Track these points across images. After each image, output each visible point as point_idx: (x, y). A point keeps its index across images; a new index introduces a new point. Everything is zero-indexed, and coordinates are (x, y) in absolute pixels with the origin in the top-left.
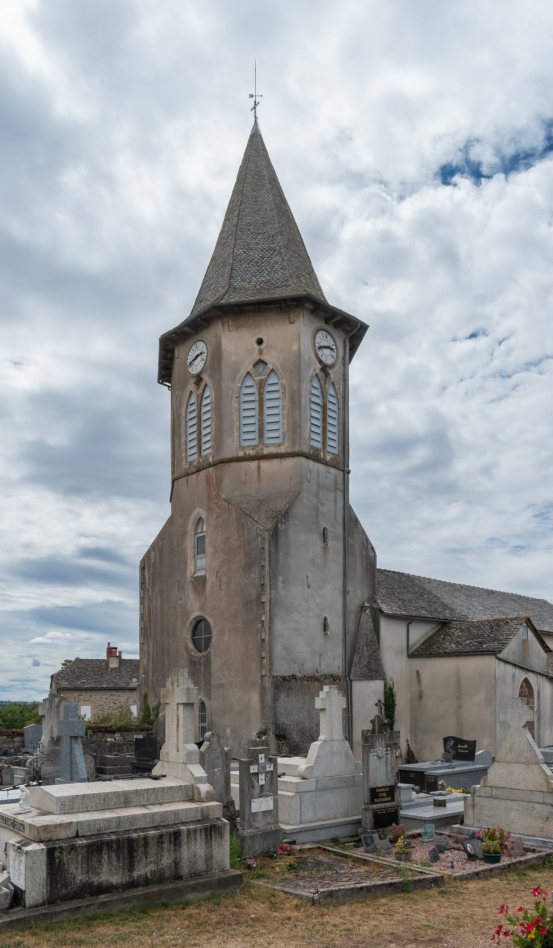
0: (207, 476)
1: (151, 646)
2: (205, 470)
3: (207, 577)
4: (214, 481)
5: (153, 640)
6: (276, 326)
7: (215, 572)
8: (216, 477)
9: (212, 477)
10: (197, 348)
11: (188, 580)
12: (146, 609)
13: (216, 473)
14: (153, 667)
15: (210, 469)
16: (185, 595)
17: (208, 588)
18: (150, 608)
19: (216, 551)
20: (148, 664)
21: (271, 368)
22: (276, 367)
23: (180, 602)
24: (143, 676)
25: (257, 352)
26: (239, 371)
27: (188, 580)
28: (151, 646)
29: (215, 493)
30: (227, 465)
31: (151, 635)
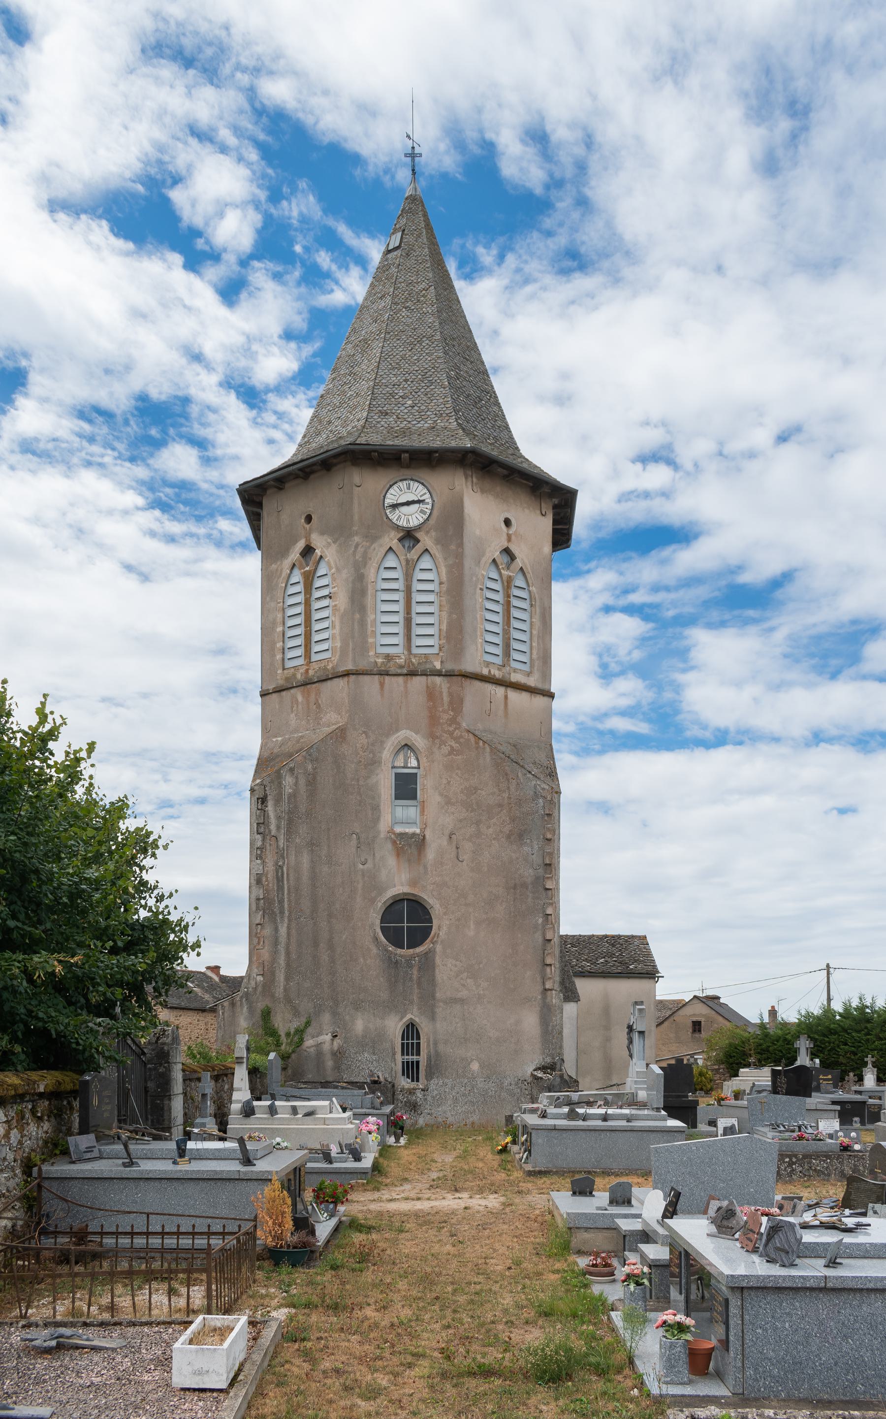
0: (427, 687)
1: (283, 930)
2: (425, 677)
3: (427, 837)
4: (446, 699)
5: (289, 920)
7: (447, 832)
8: (450, 694)
9: (441, 693)
11: (382, 835)
12: (270, 867)
13: (449, 688)
14: (288, 965)
15: (438, 680)
16: (374, 859)
17: (431, 854)
18: (281, 867)
19: (448, 802)
20: (274, 960)
23: (361, 866)
24: (260, 978)
27: (382, 835)
28: (283, 930)
29: (445, 717)
30: (468, 680)
31: (282, 912)
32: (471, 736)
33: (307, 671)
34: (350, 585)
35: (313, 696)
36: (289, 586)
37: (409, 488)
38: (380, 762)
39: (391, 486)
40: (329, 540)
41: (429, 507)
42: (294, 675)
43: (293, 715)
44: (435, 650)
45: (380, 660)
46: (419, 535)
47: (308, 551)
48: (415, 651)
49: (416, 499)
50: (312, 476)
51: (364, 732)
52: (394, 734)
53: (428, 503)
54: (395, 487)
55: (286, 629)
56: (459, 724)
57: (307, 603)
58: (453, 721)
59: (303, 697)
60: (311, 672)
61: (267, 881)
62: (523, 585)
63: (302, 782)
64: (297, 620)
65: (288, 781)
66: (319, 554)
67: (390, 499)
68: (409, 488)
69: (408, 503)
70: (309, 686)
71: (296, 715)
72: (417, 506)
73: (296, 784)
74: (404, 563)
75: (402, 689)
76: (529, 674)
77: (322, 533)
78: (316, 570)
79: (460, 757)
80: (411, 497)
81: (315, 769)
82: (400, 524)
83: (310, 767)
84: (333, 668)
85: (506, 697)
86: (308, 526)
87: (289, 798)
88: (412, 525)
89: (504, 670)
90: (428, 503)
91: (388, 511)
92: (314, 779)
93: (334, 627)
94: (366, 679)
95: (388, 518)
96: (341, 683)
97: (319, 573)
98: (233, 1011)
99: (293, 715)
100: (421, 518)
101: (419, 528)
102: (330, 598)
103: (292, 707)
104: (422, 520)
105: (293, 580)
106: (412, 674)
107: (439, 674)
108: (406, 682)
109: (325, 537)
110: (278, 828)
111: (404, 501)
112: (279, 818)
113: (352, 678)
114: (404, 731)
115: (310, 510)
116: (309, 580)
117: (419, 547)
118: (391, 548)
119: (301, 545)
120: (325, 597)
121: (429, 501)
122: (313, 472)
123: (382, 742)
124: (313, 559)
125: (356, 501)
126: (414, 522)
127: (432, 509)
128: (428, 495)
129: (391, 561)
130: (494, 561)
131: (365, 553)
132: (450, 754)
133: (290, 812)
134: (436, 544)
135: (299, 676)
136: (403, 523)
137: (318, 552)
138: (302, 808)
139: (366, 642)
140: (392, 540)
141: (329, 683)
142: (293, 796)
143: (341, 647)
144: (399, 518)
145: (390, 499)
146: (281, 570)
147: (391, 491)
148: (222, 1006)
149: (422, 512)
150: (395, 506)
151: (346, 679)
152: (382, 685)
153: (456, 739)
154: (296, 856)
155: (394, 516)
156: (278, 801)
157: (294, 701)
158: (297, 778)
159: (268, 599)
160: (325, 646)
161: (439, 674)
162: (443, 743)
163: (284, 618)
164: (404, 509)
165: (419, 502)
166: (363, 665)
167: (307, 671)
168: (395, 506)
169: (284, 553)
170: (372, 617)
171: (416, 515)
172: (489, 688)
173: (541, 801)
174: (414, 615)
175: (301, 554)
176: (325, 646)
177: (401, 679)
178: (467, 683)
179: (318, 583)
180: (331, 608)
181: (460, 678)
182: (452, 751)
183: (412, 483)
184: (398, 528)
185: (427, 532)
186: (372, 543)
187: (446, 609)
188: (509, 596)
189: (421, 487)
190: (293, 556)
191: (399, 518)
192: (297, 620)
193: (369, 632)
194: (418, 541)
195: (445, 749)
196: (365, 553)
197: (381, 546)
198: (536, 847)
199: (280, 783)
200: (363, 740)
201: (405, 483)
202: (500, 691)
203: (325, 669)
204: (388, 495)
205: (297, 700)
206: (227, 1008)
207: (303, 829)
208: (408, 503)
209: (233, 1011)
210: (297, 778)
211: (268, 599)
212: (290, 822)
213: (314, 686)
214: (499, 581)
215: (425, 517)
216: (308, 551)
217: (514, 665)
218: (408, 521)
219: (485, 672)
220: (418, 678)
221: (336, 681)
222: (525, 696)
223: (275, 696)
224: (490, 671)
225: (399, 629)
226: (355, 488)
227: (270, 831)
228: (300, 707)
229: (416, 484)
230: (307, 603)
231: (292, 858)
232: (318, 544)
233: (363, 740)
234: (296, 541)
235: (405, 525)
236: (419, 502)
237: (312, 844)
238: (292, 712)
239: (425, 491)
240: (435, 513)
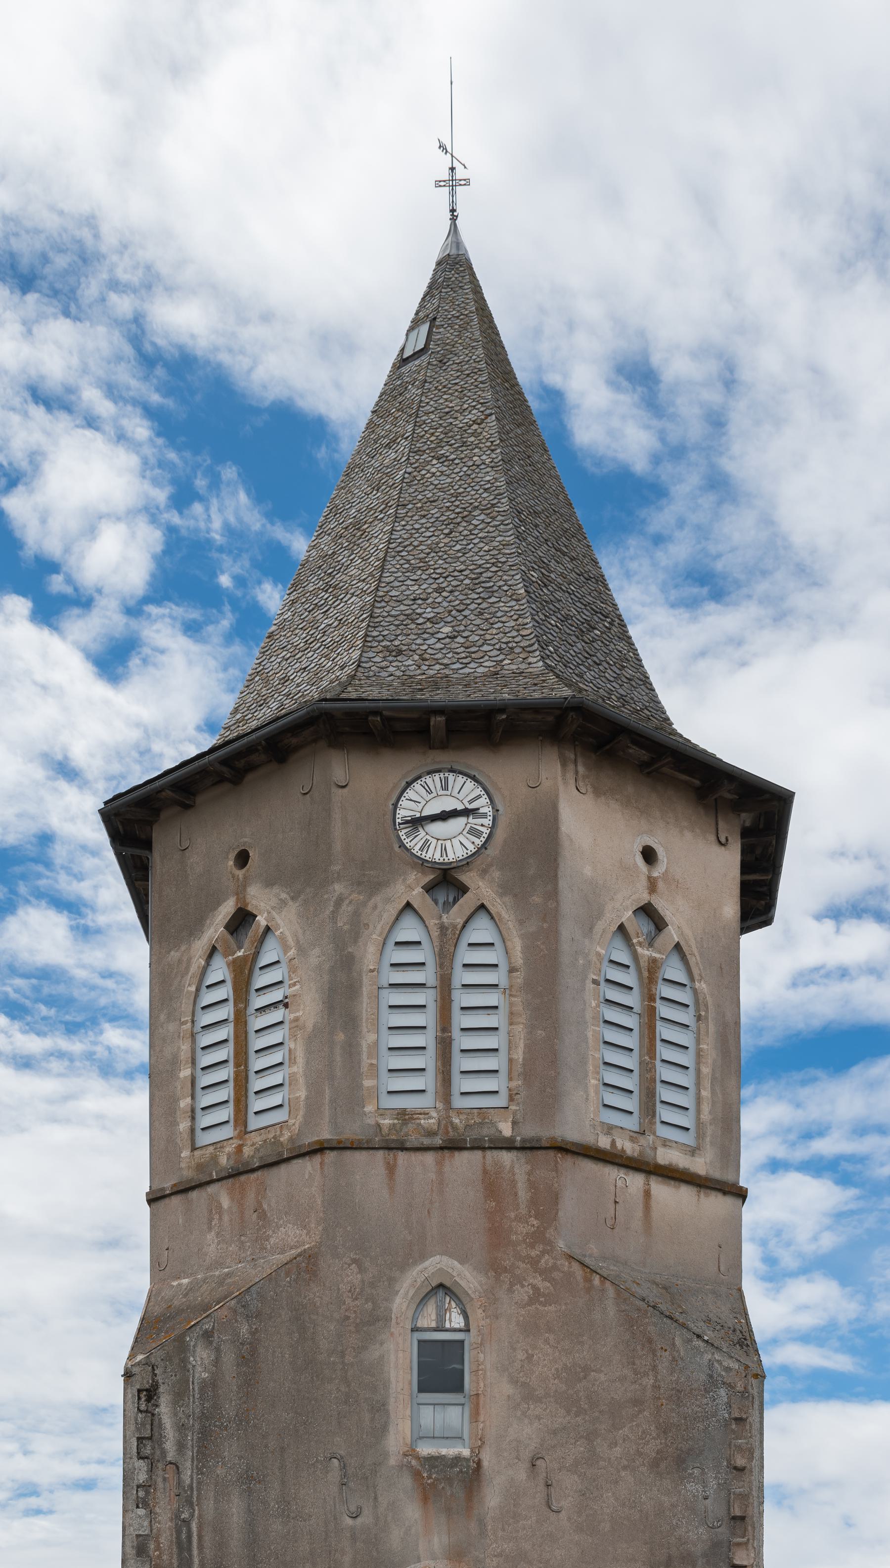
0: (485, 1172)
2: (479, 1153)
3: (485, 1464)
4: (523, 1194)
6: (688, 835)
7: (526, 1455)
8: (532, 1185)
9: (513, 1183)
11: (392, 1461)
12: (165, 1522)
13: (529, 1174)
15: (506, 1157)
16: (375, 1507)
18: (187, 1523)
19: (529, 1395)
21: (677, 940)
22: (687, 942)
23: (349, 1521)
25: (643, 883)
26: (600, 915)
27: (392, 1461)
32: (576, 1266)
33: (239, 1149)
34: (326, 977)
36: (204, 989)
37: (445, 787)
38: (388, 1319)
39: (409, 784)
40: (284, 896)
41: (488, 822)
42: (214, 1158)
43: (211, 1236)
44: (500, 1101)
45: (386, 1122)
46: (465, 878)
48: (459, 1102)
49: (460, 807)
50: (250, 777)
51: (355, 1261)
52: (415, 1263)
53: (484, 815)
54: (417, 786)
55: (199, 1072)
56: (550, 1245)
57: (240, 1020)
58: (538, 1237)
59: (232, 1199)
60: (247, 1151)
61: (158, 1548)
62: (681, 977)
63: (229, 1359)
64: (221, 1054)
67: (408, 808)
68: (445, 787)
69: (444, 816)
70: (243, 1178)
72: (461, 821)
73: (217, 1362)
74: (435, 933)
75: (433, 1176)
76: (693, 1151)
78: (256, 954)
79: (552, 1308)
80: (450, 804)
81: (253, 1333)
82: (428, 856)
83: (244, 1329)
84: (291, 1139)
85: (647, 1194)
87: (202, 1389)
88: (451, 857)
89: (642, 1140)
90: (484, 815)
91: (402, 834)
92: (253, 1352)
93: (293, 1061)
94: (360, 1157)
95: (402, 845)
96: (308, 1167)
97: (264, 960)
99: (211, 1236)
100: (471, 845)
101: (466, 863)
102: (286, 1006)
103: (210, 1220)
104: (472, 849)
105: (211, 979)
106: (453, 1146)
107: (508, 1145)
108: (440, 1164)
110: (181, 1446)
111: (437, 811)
112: (181, 1428)
113: (330, 1156)
114: (437, 1258)
115: (245, 841)
117: (468, 902)
118: (408, 905)
120: (275, 1005)
121: (488, 810)
122: (251, 768)
123: (392, 1281)
124: (251, 933)
125: (337, 816)
126: (456, 852)
127: (493, 827)
128: (484, 800)
129: (409, 930)
130: (621, 928)
131: (356, 914)
132: (531, 1301)
133: (204, 1417)
134: (501, 895)
135: (223, 1160)
136: (433, 854)
138: (230, 1409)
139: (360, 1086)
140: (411, 888)
141: (283, 1169)
142: (211, 1385)
143: (307, 1098)
144: (426, 845)
145: (408, 808)
147: (410, 794)
149: (474, 832)
150: (417, 823)
151: (317, 1159)
152: (391, 1169)
153: (545, 1273)
154: (216, 1501)
155: (415, 843)
156: (180, 1395)
158: (218, 1350)
160: (275, 1099)
161: (508, 1145)
162: (520, 1280)
163: (193, 1052)
164: (437, 829)
165: (466, 812)
166: (352, 1131)
167: (239, 1149)
168: (417, 823)
170: (371, 1037)
171: (461, 838)
172: (612, 1174)
173: (723, 1392)
174: (456, 1033)
175: (227, 927)
176: (275, 1099)
177: (429, 1158)
178: (567, 1163)
179: (262, 979)
180: (286, 1026)
181: (551, 1153)
182: (536, 1296)
183: (451, 777)
184: (423, 864)
185: (484, 872)
186: (370, 896)
187: (522, 1019)
188: (652, 998)
189: (470, 784)
191: (426, 845)
192: (221, 1054)
193: (364, 1068)
194: (463, 889)
195: (522, 1293)
196: (356, 914)
197: (388, 900)
198: (713, 1483)
199: (184, 1361)
200: (353, 1276)
201: (437, 777)
202: (635, 1181)
204: (403, 803)
205: (220, 1206)
207: (231, 1449)
208: (444, 816)
210: (218, 1350)
212: (205, 1435)
214: (632, 969)
215: (479, 842)
217: (664, 1132)
218: (444, 850)
219: (604, 1142)
220: (466, 1154)
221: (297, 1164)
222: (686, 1193)
223: (176, 1200)
224: (613, 1143)
225: (427, 1061)
226: (334, 790)
227: (164, 1453)
228: (226, 1218)
229: (461, 779)
230: (240, 1020)
231: (209, 1506)
233: (353, 1276)
235: (437, 857)
236: (466, 812)
237: (251, 1478)
238: (210, 1229)
239: (479, 791)
240: (501, 835)
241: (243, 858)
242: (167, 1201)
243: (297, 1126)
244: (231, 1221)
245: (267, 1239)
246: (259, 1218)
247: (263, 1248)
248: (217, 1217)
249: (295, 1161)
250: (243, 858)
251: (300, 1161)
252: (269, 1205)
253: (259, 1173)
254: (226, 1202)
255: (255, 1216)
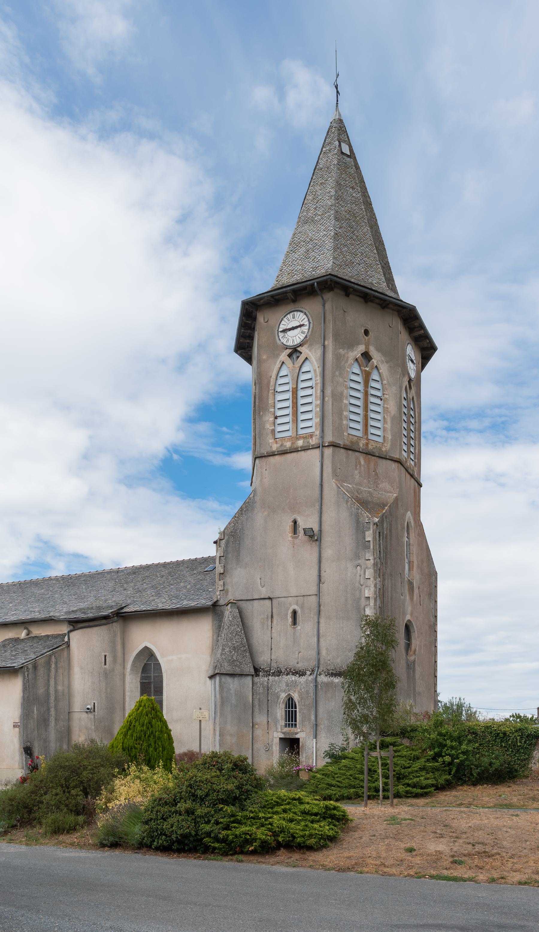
10: (294, 318)
33: (367, 444)
35: (372, 465)
42: (358, 443)
47: (366, 356)
59: (365, 462)
60: (370, 447)
65: (385, 525)
66: (375, 364)
70: (369, 456)
71: (359, 473)
77: (379, 350)
84: (386, 451)
86: (367, 338)
98: (35, 674)
99: (356, 472)
102: (381, 400)
103: (356, 466)
109: (380, 354)
112: (383, 551)
116: (367, 377)
119: (362, 348)
120: (378, 397)
135: (361, 445)
137: (375, 361)
141: (384, 461)
143: (391, 439)
146: (348, 358)
148: (28, 668)
157: (358, 462)
159: (337, 373)
167: (367, 444)
169: (351, 345)
190: (356, 352)
199: (383, 524)
203: (380, 449)
206: (31, 670)
209: (35, 674)
211: (337, 373)
213: (373, 458)
216: (366, 356)
223: (342, 451)
228: (362, 468)
232: (375, 356)
234: (358, 344)
238: (356, 469)
241: (366, 332)
242: (339, 449)
243: (388, 447)
244: (364, 470)
245: (379, 484)
246: (375, 474)
247: (377, 487)
248: (359, 466)
249: (389, 461)
250: (366, 332)
251: (390, 461)
252: (379, 472)
253: (375, 458)
254: (362, 462)
255: (374, 473)
